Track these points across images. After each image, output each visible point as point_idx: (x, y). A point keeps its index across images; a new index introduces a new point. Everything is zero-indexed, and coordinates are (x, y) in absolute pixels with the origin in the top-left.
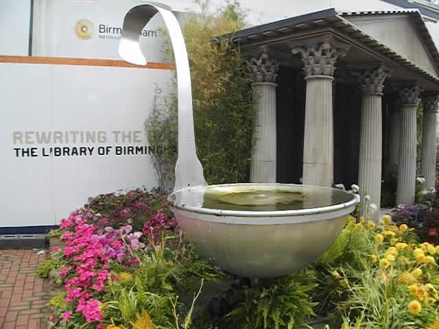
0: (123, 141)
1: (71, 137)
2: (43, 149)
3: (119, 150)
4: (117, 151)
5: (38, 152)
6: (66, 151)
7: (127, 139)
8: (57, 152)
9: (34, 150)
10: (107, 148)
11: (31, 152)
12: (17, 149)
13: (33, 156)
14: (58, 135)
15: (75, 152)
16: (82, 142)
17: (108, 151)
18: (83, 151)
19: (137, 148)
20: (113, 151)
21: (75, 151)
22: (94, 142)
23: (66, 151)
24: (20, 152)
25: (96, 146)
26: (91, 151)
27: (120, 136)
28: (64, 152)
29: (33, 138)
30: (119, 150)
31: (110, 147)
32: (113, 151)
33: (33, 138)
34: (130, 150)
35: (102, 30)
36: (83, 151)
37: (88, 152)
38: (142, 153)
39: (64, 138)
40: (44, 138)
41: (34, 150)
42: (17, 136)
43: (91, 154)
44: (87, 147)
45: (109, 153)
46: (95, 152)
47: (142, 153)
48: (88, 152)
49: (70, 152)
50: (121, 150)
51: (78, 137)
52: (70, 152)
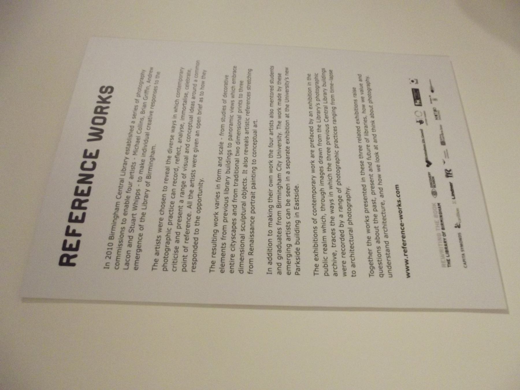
0: (439, 227)
1: (440, 246)
3: (443, 229)
5: (448, 258)
6: (446, 248)
7: (438, 226)
8: (447, 252)
11: (449, 261)
14: (441, 251)
15: (446, 245)
16: (441, 242)
18: (445, 242)
20: (444, 231)
22: (441, 238)
23: (446, 248)
25: (442, 237)
26: (445, 239)
27: (438, 228)
29: (443, 260)
30: (443, 229)
32: (444, 231)
33: (443, 260)
34: (442, 224)
35: (280, 206)
36: (445, 242)
39: (442, 249)
40: (443, 256)
42: (443, 266)
46: (445, 237)
51: (440, 244)
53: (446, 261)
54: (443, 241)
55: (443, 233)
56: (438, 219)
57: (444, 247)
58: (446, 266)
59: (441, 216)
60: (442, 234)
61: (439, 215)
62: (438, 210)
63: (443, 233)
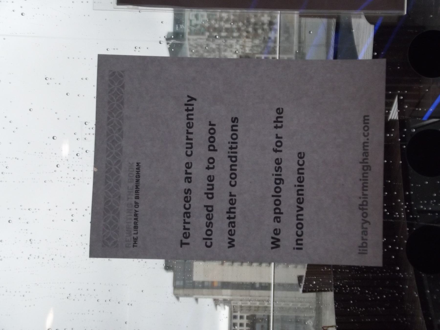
2: (134, 234)
3: (137, 198)
4: (137, 199)
5: (135, 236)
8: (136, 227)
9: (135, 238)
10: (135, 203)
11: (135, 240)
12: (134, 246)
13: (137, 239)
17: (137, 203)
18: (136, 215)
19: (136, 188)
20: (137, 201)
21: (136, 219)
24: (135, 245)
26: (136, 211)
28: (136, 224)
30: (137, 198)
31: (135, 201)
32: (137, 201)
34: (137, 192)
36: (136, 215)
37: (137, 213)
38: (139, 186)
41: (135, 238)
43: (138, 211)
44: (134, 213)
45: (138, 202)
46: (137, 209)
47: (139, 186)
48: (137, 213)
49: (136, 221)
50: (137, 197)
52: (136, 221)
53: (133, 240)
54: (133, 214)
55: (136, 203)
56: (133, 184)
57: (133, 221)
58: (132, 245)
59: (138, 181)
60: (134, 204)
61: (135, 178)
62: (135, 173)
63: (136, 203)
